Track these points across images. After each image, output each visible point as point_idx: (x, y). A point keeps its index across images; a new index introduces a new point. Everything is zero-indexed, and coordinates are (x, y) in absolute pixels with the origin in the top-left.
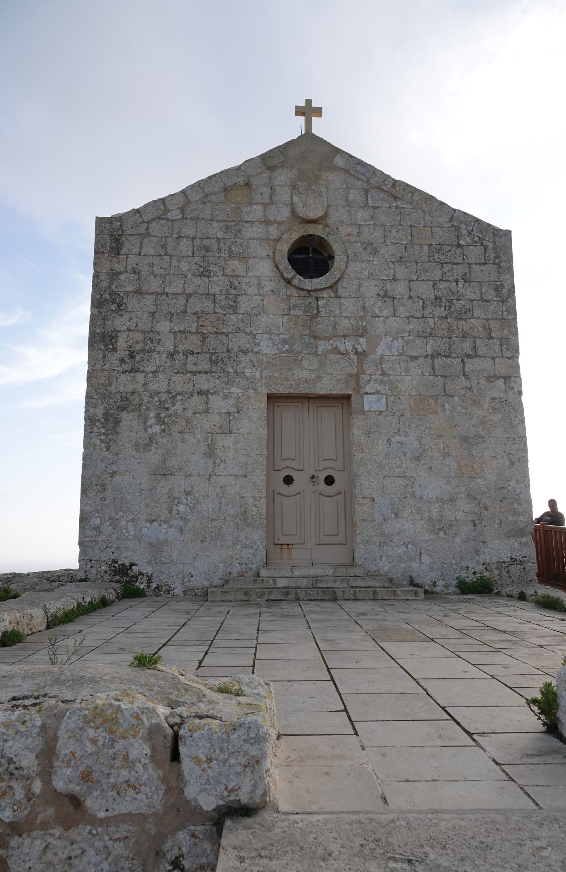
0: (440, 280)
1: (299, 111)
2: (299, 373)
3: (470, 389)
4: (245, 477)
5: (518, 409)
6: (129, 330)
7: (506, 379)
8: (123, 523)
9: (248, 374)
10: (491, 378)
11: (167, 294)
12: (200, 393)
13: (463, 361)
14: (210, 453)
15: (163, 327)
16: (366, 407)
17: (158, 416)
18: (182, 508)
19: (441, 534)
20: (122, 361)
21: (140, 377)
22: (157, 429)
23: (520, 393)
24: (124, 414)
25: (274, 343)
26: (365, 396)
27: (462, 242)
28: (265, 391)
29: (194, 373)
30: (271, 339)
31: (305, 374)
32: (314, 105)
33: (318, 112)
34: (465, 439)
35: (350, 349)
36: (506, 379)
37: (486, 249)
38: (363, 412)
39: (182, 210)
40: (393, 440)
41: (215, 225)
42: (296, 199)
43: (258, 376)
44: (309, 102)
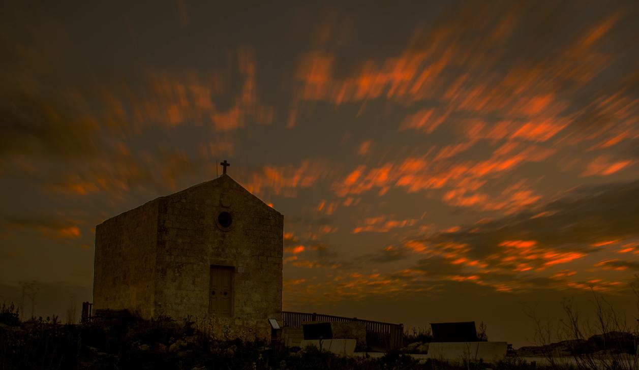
0: (263, 230)
1: (222, 164)
2: (220, 259)
3: (268, 267)
4: (203, 291)
5: (281, 274)
6: (169, 241)
7: (279, 264)
8: (168, 304)
9: (205, 257)
10: (275, 264)
11: (181, 229)
12: (191, 263)
13: (267, 258)
14: (194, 283)
15: (180, 241)
16: (239, 271)
17: (178, 270)
18: (185, 301)
19: (258, 312)
20: (167, 251)
21: (173, 257)
22: (178, 275)
23: (282, 269)
24: (168, 269)
25: (213, 248)
26: (239, 268)
27: (270, 218)
28: (209, 264)
29: (189, 257)
30: (212, 247)
31: (222, 259)
32: (227, 163)
33: (229, 165)
34: (266, 282)
35: (235, 252)
36: (279, 264)
37: (276, 221)
38: (238, 273)
39: (185, 199)
40: (246, 282)
41: (196, 205)
42: (222, 199)
43: (208, 259)
44: (225, 161)
